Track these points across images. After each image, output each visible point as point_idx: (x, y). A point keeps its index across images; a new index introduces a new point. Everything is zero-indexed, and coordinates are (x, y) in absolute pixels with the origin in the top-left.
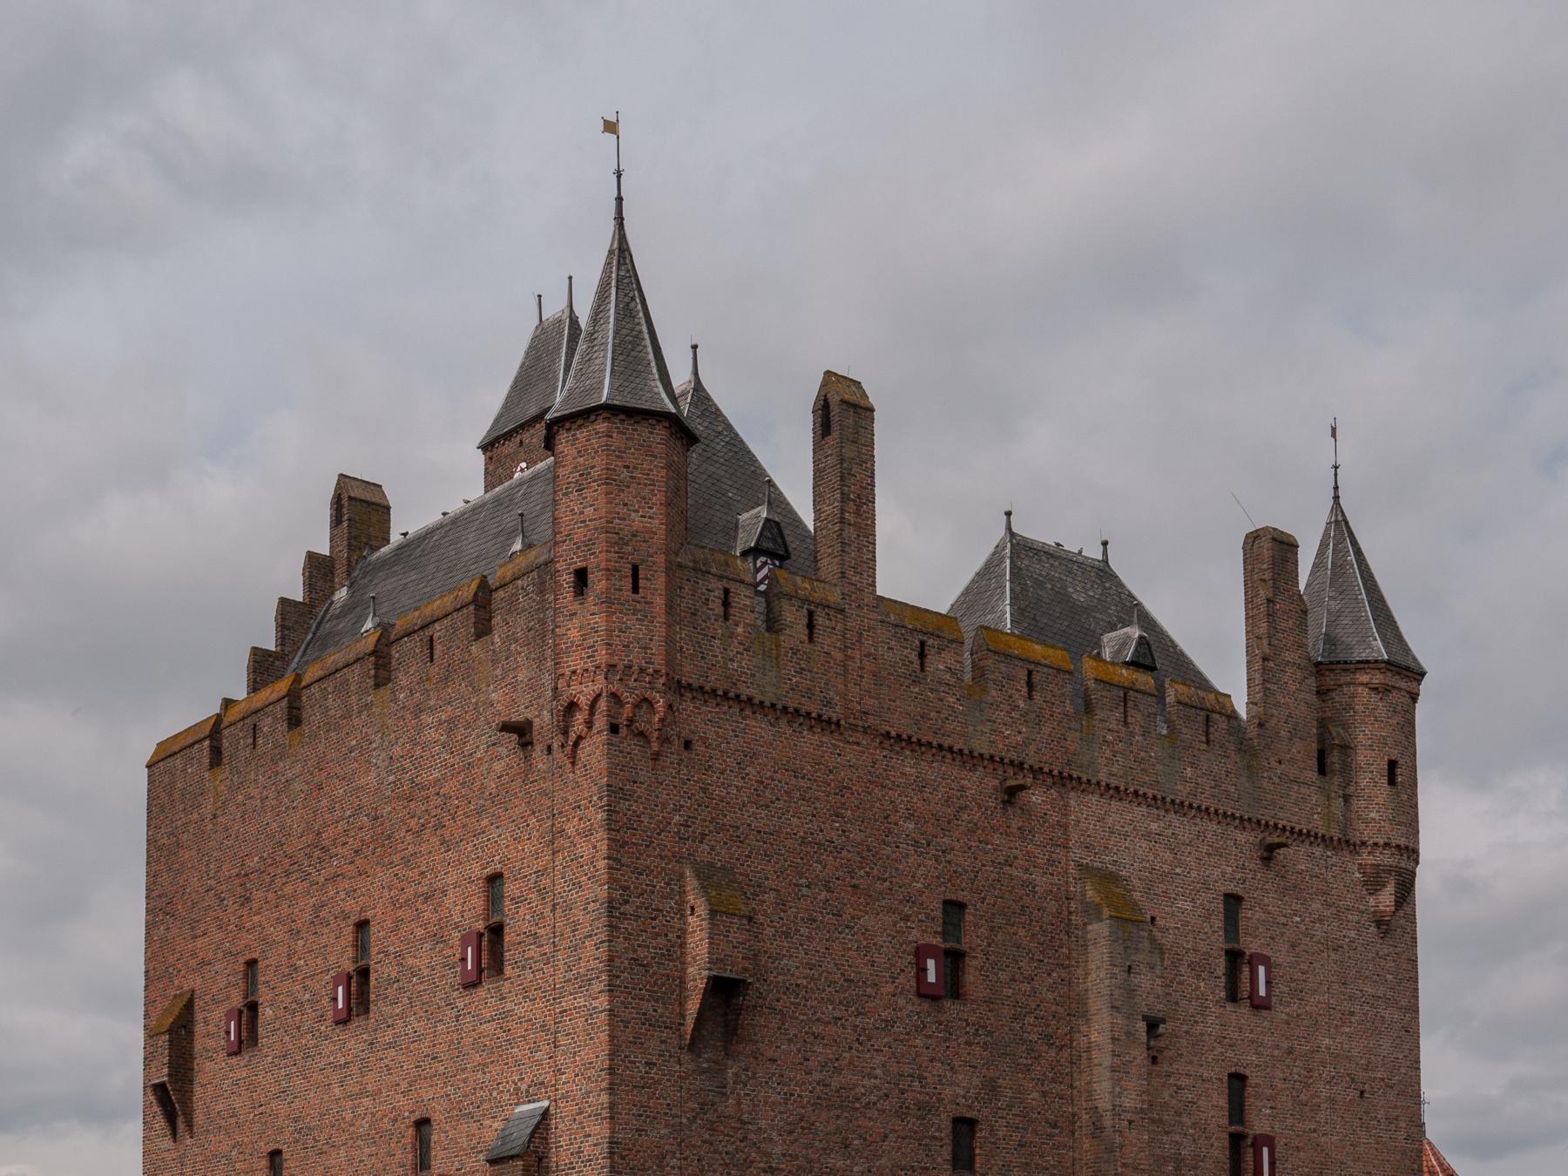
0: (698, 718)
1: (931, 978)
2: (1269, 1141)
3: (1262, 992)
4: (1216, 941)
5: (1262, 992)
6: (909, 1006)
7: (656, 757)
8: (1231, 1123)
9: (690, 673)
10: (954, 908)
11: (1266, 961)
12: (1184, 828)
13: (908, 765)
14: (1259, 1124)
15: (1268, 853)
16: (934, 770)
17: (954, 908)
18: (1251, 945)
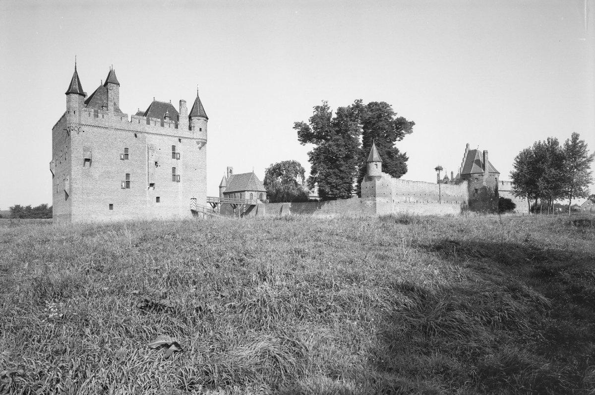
0: (83, 128)
1: (122, 157)
2: (179, 176)
3: (178, 157)
4: (171, 152)
5: (178, 157)
6: (119, 161)
7: (78, 133)
8: (173, 173)
9: (83, 123)
10: (126, 149)
11: (179, 154)
12: (166, 138)
13: (119, 132)
14: (177, 173)
15: (180, 140)
16: (124, 132)
17: (126, 149)
18: (176, 152)
